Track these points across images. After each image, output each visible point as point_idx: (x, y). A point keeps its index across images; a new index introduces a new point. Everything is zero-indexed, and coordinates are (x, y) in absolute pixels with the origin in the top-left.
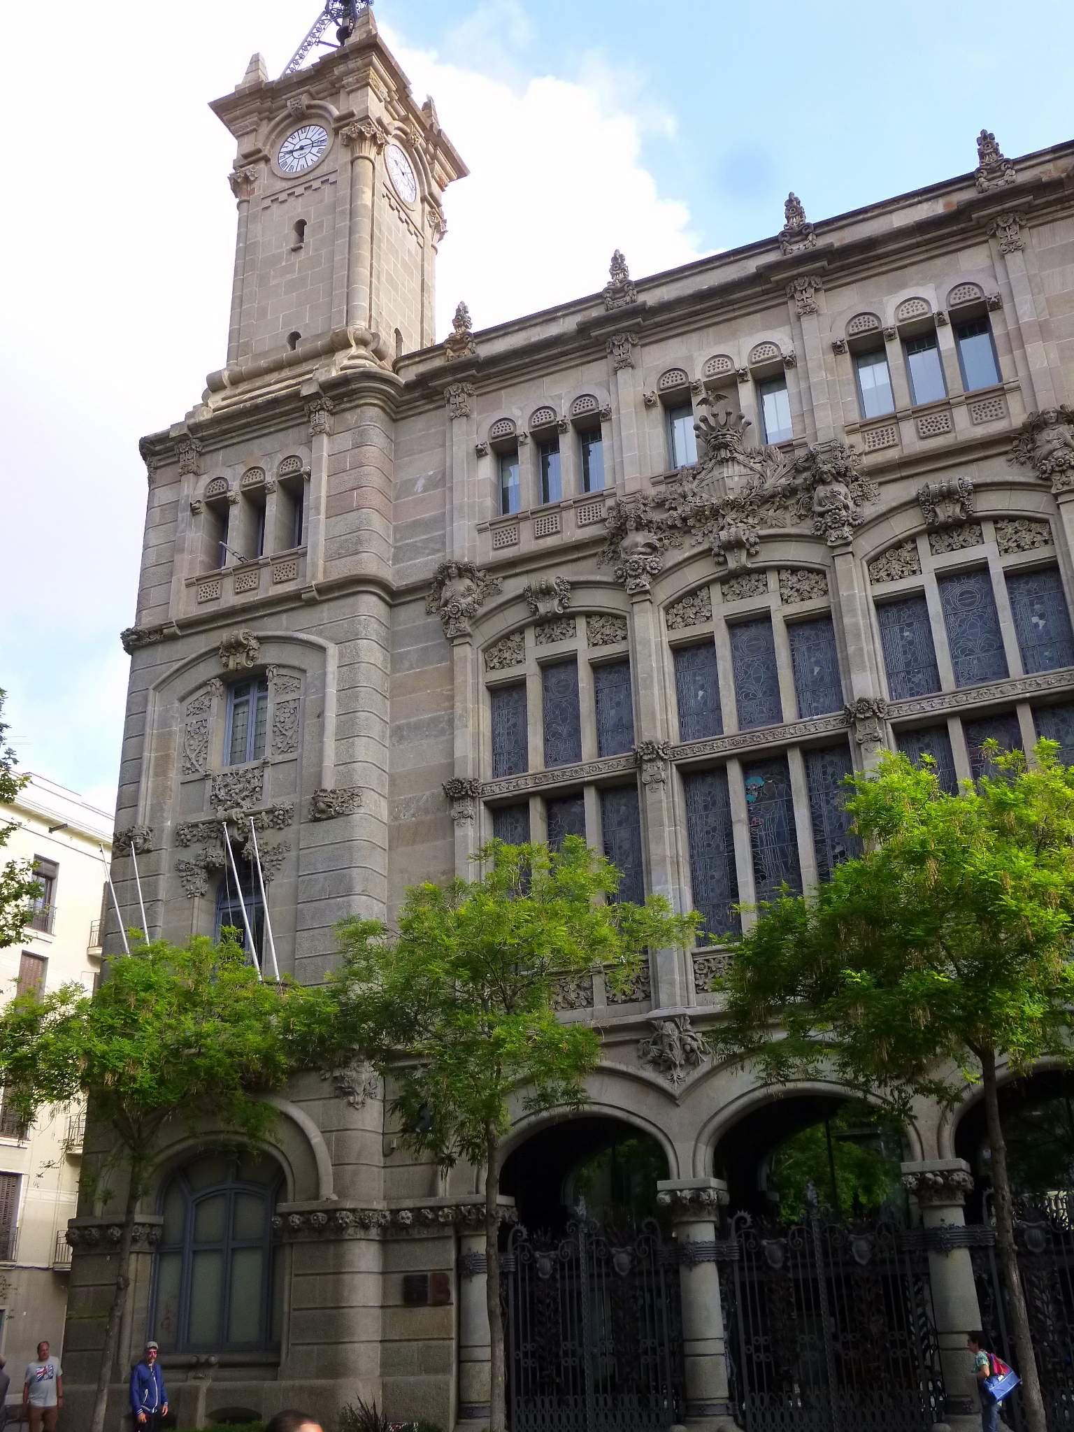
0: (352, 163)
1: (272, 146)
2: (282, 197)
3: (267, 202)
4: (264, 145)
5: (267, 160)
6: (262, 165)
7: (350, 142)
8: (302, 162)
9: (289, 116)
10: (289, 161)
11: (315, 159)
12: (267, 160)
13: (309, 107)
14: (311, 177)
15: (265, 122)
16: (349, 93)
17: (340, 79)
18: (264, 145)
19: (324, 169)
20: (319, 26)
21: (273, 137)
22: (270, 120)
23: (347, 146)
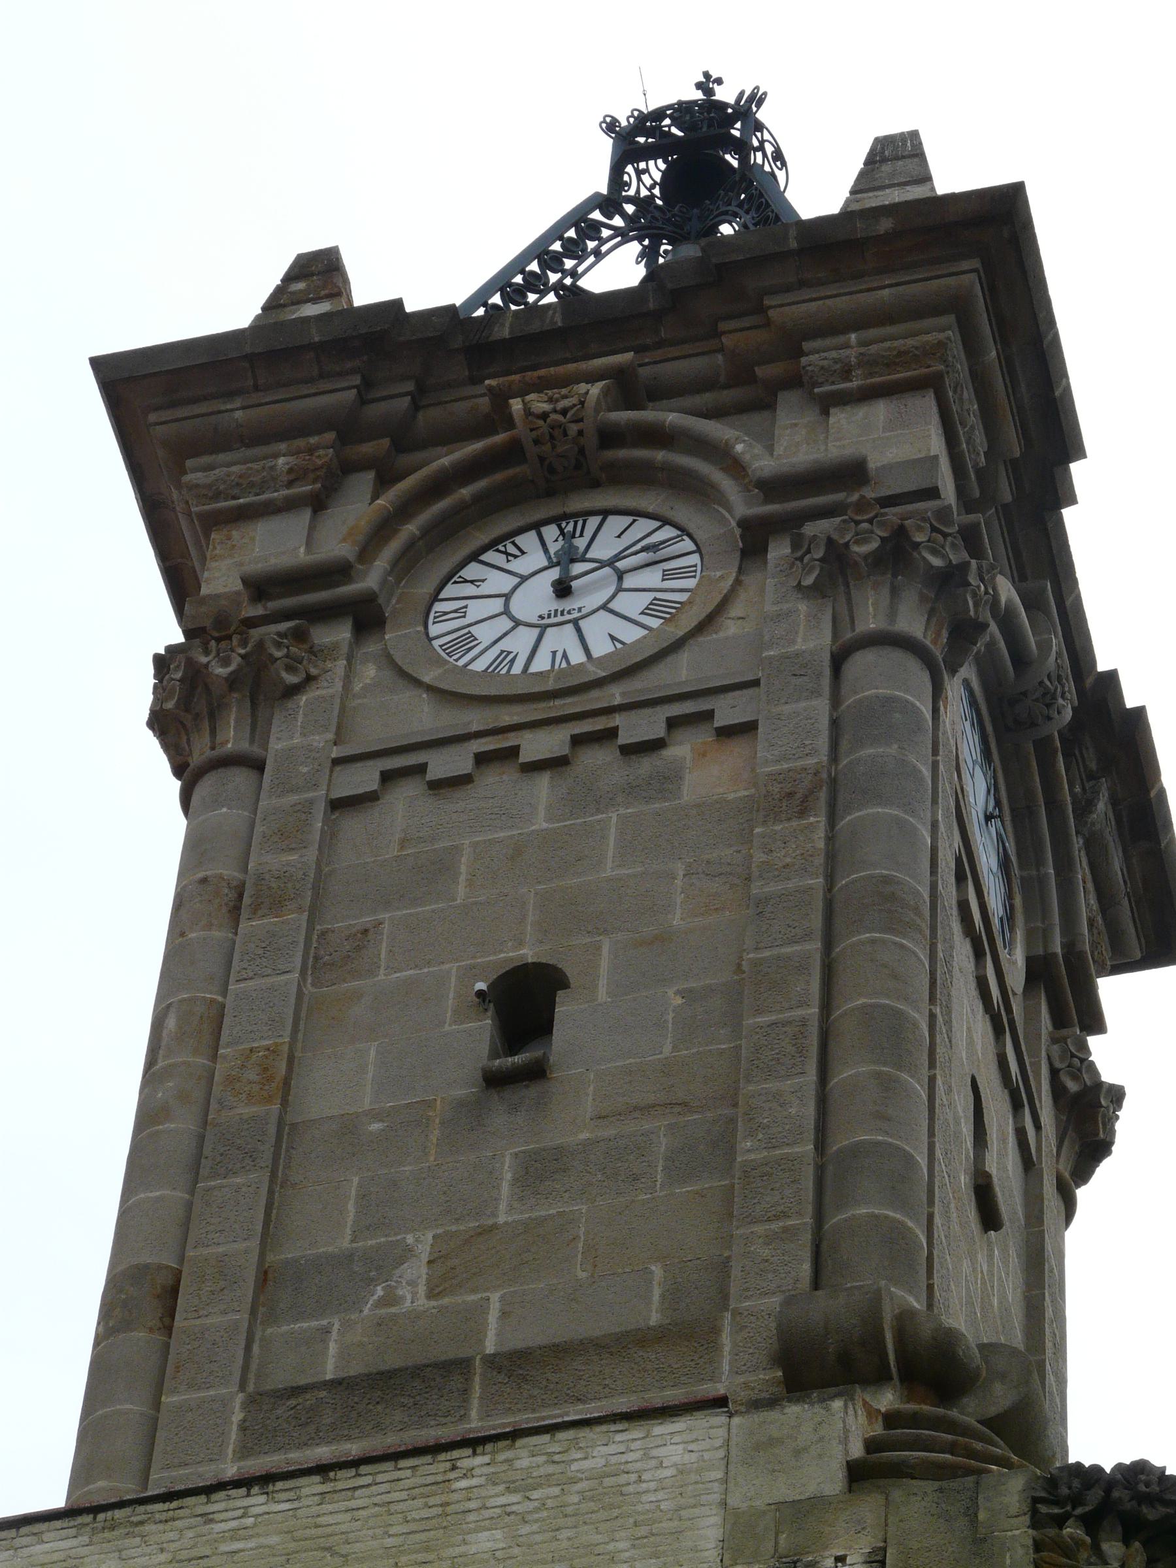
0: (838, 661)
1: (408, 563)
2: (458, 761)
3: (365, 778)
4: (367, 552)
5: (367, 618)
6: (340, 634)
7: (836, 573)
8: (562, 640)
9: (512, 453)
10: (486, 634)
11: (631, 634)
12: (367, 618)
13: (610, 437)
14: (616, 694)
15: (370, 476)
16: (826, 404)
17: (792, 344)
18: (367, 552)
19: (681, 672)
20: (579, 233)
21: (411, 528)
22: (384, 481)
23: (817, 591)
